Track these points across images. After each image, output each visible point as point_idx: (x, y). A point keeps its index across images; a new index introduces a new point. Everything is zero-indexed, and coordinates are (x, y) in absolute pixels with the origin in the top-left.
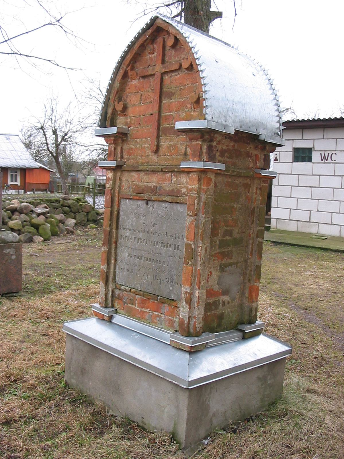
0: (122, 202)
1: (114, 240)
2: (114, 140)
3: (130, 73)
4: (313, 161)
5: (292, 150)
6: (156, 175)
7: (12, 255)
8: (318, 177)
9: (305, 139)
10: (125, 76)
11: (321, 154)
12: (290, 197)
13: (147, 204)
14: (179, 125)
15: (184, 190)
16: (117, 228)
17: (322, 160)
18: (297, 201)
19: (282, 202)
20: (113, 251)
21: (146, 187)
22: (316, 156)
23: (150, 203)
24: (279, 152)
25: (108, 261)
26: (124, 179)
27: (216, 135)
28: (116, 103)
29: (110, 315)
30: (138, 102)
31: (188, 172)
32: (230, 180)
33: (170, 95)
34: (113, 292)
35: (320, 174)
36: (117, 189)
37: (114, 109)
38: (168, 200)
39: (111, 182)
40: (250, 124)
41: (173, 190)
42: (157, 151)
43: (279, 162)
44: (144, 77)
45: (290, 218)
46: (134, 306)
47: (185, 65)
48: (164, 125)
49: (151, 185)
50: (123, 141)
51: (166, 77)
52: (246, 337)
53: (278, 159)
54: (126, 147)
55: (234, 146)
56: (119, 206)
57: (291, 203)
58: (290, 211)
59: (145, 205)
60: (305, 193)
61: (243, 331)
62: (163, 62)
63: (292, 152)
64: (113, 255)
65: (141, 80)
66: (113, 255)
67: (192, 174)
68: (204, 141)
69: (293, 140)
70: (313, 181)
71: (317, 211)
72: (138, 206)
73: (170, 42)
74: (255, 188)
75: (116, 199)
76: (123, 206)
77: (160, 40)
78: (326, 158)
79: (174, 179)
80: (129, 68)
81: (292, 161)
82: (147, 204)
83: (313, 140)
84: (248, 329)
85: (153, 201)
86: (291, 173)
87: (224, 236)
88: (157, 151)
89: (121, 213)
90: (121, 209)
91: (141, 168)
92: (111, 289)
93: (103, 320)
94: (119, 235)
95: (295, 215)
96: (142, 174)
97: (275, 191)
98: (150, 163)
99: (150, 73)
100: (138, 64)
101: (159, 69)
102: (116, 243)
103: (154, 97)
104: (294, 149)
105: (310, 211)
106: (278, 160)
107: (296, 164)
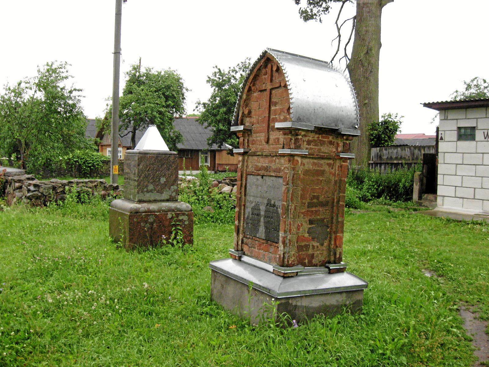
0: (249, 177)
1: (243, 203)
2: (243, 134)
3: (253, 88)
4: (477, 139)
5: (456, 129)
6: (267, 158)
7: (185, 221)
8: (482, 155)
9: (469, 119)
10: (250, 90)
11: (484, 132)
12: (456, 175)
13: (262, 178)
14: (278, 125)
15: (283, 168)
16: (245, 195)
17: (485, 138)
20: (243, 211)
21: (262, 166)
22: (479, 135)
23: (264, 177)
25: (239, 218)
26: (249, 161)
27: (300, 132)
28: (244, 108)
29: (240, 255)
30: (258, 108)
31: (283, 155)
32: (315, 161)
33: (276, 104)
34: (242, 240)
36: (245, 168)
37: (243, 113)
38: (274, 175)
39: (241, 164)
40: (330, 122)
41: (277, 169)
42: (267, 142)
43: (445, 141)
44: (261, 91)
46: (254, 249)
47: (282, 85)
48: (272, 125)
49: (265, 165)
50: (248, 135)
51: (273, 92)
52: (331, 272)
54: (251, 139)
55: (318, 137)
56: (246, 180)
57: (457, 181)
59: (261, 179)
61: (328, 268)
62: (271, 81)
63: (456, 132)
64: (242, 214)
65: (259, 93)
66: (242, 214)
67: (285, 157)
68: (293, 135)
69: (457, 119)
70: (477, 159)
72: (258, 179)
73: (275, 69)
74: (337, 166)
75: (244, 175)
76: (249, 180)
77: (269, 66)
79: (277, 161)
80: (251, 85)
81: (456, 140)
82: (262, 178)
83: (476, 119)
84: (332, 267)
85: (266, 176)
86: (455, 151)
87: (312, 199)
88: (267, 142)
89: (248, 185)
90: (248, 182)
91: (258, 153)
92: (241, 238)
93: (236, 259)
94: (247, 201)
96: (260, 157)
97: (441, 169)
98: (265, 150)
99: (263, 88)
100: (258, 82)
101: (269, 87)
102: (244, 205)
103: (266, 104)
104: (459, 128)
105: (475, 188)
107: (461, 143)
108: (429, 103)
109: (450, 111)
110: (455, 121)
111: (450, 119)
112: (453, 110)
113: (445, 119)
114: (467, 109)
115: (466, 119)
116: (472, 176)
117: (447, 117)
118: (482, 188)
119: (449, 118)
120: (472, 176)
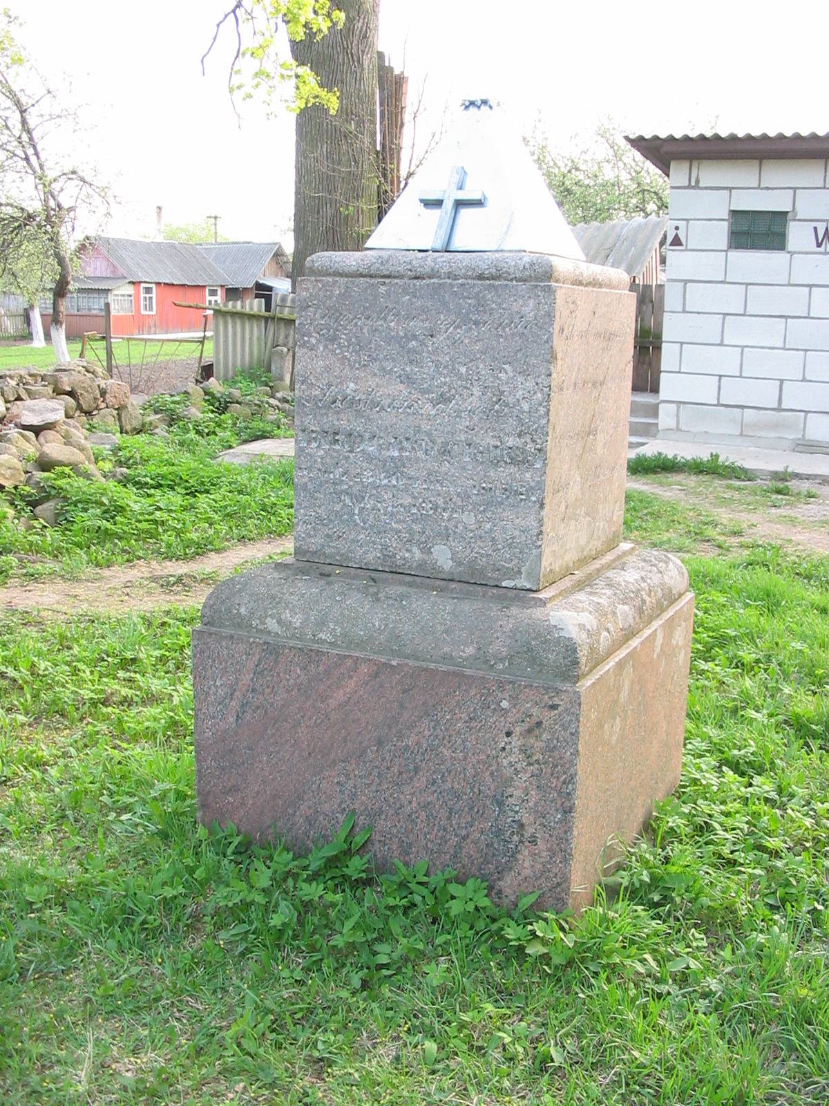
4: (791, 245)
8: (807, 289)
9: (767, 188)
11: (815, 229)
12: (721, 344)
17: (819, 245)
18: (742, 353)
19: (695, 358)
22: (799, 236)
24: (685, 222)
35: (811, 283)
43: (686, 250)
45: (718, 400)
53: (683, 240)
57: (726, 361)
58: (719, 381)
60: (772, 333)
63: (726, 224)
69: (730, 189)
70: (793, 301)
71: (802, 381)
78: (820, 241)
81: (725, 248)
86: (722, 279)
95: (734, 392)
104: (734, 213)
105: (782, 381)
106: (681, 245)
107: (736, 255)
108: (641, 139)
109: (705, 163)
110: (726, 192)
111: (706, 188)
112: (800, 160)
113: (689, 187)
114: (764, 161)
115: (759, 188)
116: (773, 348)
117: (697, 181)
118: (804, 380)
119: (701, 185)
120: (773, 348)
